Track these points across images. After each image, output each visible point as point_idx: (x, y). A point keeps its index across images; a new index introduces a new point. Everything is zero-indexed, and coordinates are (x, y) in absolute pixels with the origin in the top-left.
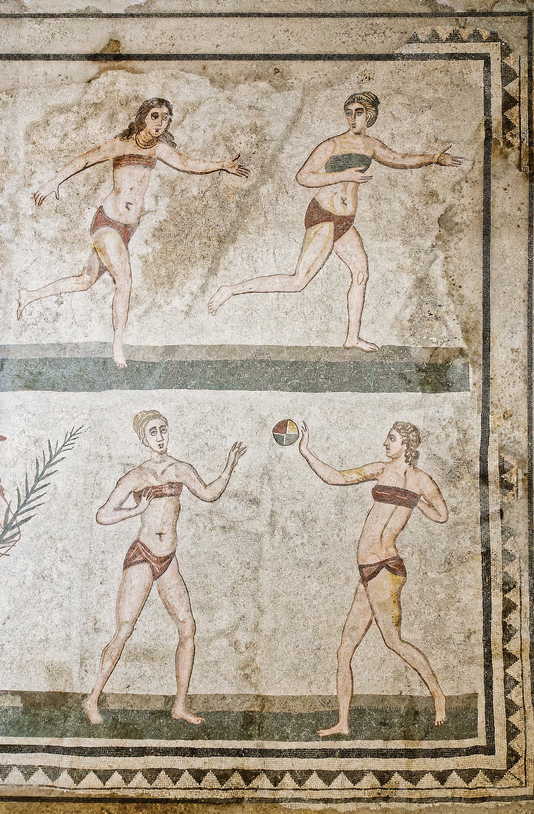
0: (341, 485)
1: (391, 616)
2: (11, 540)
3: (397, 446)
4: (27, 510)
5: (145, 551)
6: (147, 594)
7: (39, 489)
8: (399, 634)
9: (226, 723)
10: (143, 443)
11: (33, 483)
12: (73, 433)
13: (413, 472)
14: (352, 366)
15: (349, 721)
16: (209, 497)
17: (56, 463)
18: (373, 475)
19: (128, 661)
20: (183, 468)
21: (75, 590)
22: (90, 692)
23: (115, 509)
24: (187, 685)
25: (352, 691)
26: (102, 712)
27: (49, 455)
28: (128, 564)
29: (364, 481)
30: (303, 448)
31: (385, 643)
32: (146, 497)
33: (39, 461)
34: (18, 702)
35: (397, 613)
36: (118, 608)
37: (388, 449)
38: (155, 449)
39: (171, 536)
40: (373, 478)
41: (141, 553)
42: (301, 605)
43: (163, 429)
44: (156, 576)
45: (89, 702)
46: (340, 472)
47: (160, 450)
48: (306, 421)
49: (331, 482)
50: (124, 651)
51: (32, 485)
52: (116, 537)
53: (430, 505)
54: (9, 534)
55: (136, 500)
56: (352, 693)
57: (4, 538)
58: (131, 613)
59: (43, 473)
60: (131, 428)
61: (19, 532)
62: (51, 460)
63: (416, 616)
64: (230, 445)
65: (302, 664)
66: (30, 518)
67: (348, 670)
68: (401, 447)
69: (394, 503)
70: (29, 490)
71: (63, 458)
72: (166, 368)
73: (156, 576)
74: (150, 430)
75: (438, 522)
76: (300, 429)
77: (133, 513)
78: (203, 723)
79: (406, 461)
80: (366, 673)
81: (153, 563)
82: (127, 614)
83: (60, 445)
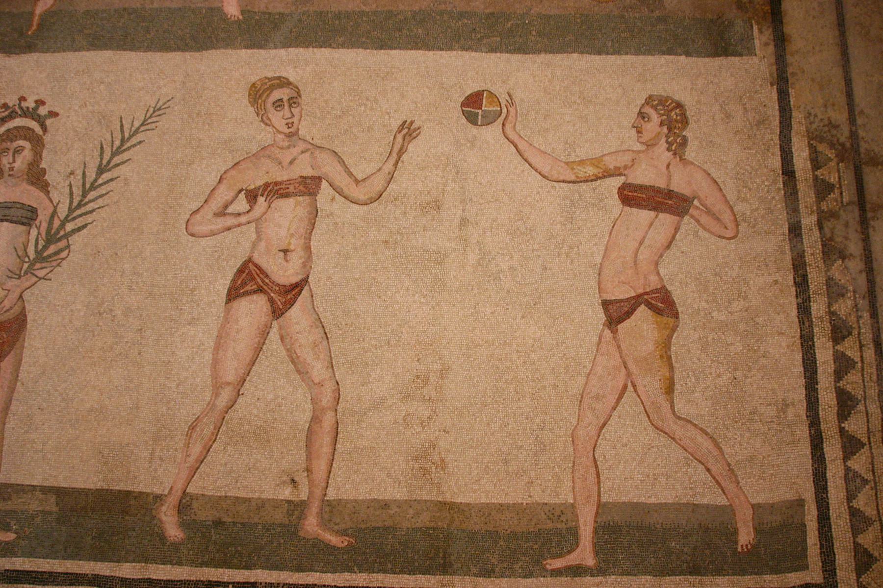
0: (569, 182)
1: (657, 378)
2: (55, 258)
3: (653, 127)
4: (80, 216)
5: (261, 275)
6: (262, 341)
8: (672, 407)
9: (389, 547)
10: (262, 121)
11: (94, 176)
12: (158, 107)
13: (681, 166)
14: (579, 20)
15: (595, 545)
16: (362, 198)
17: (129, 148)
18: (619, 168)
19: (228, 444)
20: (324, 158)
21: (148, 333)
22: (166, 492)
24: (324, 485)
25: (599, 496)
26: (183, 525)
27: (120, 137)
28: (234, 294)
29: (604, 177)
31: (650, 421)
32: (265, 196)
33: (105, 146)
34: (51, 505)
35: (667, 374)
36: (215, 363)
37: (639, 132)
38: (281, 129)
39: (302, 253)
40: (616, 172)
41: (254, 279)
42: (511, 361)
43: (293, 102)
44: (277, 312)
45: (164, 508)
46: (567, 163)
47: (287, 131)
48: (511, 91)
49: (554, 178)
50: (223, 428)
51: (92, 179)
52: (216, 255)
53: (709, 212)
54: (52, 249)
55: (249, 202)
56: (599, 500)
57: (45, 254)
58: (236, 369)
59: (109, 162)
60: (246, 101)
61: (68, 246)
62: (122, 145)
63: (697, 379)
64: (395, 124)
65: (515, 452)
67: (590, 463)
68: (658, 129)
69: (654, 209)
70: (88, 186)
71: (140, 142)
72: (300, 21)
73: (277, 312)
74: (273, 104)
75: (724, 238)
76: (503, 103)
77: (243, 219)
78: (350, 544)
79: (668, 150)
80: (621, 467)
81: (272, 295)
82: (230, 374)
83: (137, 124)
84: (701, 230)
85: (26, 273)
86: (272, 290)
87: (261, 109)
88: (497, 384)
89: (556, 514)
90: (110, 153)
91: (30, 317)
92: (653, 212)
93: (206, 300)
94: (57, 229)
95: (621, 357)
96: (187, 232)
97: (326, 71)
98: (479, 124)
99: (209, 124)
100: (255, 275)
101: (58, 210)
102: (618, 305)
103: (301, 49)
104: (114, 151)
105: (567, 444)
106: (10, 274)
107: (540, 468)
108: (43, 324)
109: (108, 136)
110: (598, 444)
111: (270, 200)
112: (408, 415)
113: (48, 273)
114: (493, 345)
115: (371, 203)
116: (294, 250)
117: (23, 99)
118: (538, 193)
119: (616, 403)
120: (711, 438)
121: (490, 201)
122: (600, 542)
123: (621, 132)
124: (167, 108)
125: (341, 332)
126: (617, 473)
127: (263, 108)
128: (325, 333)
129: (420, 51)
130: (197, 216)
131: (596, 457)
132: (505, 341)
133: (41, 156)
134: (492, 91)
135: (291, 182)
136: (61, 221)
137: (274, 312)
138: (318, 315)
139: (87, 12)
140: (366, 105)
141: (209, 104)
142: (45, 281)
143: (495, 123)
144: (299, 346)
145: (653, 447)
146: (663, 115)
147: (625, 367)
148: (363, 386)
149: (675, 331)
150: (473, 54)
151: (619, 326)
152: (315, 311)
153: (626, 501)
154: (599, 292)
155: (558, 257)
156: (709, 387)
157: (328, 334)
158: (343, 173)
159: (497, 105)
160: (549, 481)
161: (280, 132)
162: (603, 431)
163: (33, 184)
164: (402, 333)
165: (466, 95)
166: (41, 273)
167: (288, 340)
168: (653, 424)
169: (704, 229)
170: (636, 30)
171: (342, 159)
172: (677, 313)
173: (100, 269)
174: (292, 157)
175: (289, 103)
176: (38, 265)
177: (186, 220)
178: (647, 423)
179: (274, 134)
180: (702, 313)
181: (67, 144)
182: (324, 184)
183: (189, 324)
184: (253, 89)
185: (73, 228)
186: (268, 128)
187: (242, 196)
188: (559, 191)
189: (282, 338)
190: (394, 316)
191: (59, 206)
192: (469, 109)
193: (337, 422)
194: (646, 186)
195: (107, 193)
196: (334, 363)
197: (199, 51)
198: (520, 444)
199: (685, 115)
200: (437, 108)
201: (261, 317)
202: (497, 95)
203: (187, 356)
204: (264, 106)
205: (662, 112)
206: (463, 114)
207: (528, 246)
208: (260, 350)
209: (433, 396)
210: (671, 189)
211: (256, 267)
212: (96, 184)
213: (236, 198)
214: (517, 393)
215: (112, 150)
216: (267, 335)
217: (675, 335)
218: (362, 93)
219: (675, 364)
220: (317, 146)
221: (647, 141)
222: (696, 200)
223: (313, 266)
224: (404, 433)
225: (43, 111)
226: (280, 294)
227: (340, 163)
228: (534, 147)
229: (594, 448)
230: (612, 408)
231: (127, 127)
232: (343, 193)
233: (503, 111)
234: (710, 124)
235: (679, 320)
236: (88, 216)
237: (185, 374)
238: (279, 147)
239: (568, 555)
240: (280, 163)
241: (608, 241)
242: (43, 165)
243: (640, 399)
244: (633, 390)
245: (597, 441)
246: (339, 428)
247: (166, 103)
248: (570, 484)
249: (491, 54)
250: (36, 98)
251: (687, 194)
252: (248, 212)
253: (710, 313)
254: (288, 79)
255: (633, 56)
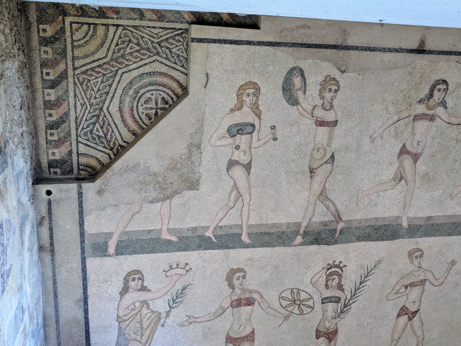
4: (354, 298)
10: (411, 263)
11: (359, 285)
17: (370, 275)
23: (395, 294)
28: (399, 315)
38: (417, 265)
41: (404, 311)
43: (421, 256)
44: (410, 319)
47: (417, 265)
51: (358, 286)
52: (394, 305)
54: (346, 309)
57: (343, 311)
59: (363, 280)
62: (368, 274)
64: (450, 261)
66: (356, 301)
70: (357, 289)
71: (373, 273)
73: (410, 319)
77: (403, 294)
82: (396, 337)
83: (372, 267)
85: (337, 317)
91: (339, 330)
101: (347, 297)
106: (332, 318)
109: (363, 272)
117: (334, 261)
133: (341, 280)
137: (409, 319)
139: (356, 228)
140: (442, 255)
161: (416, 266)
163: (339, 290)
166: (342, 317)
176: (341, 314)
181: (350, 276)
182: (427, 281)
187: (403, 287)
189: (411, 326)
225: (342, 265)
226: (411, 314)
231: (369, 268)
237: (384, 339)
242: (342, 283)
250: (339, 261)
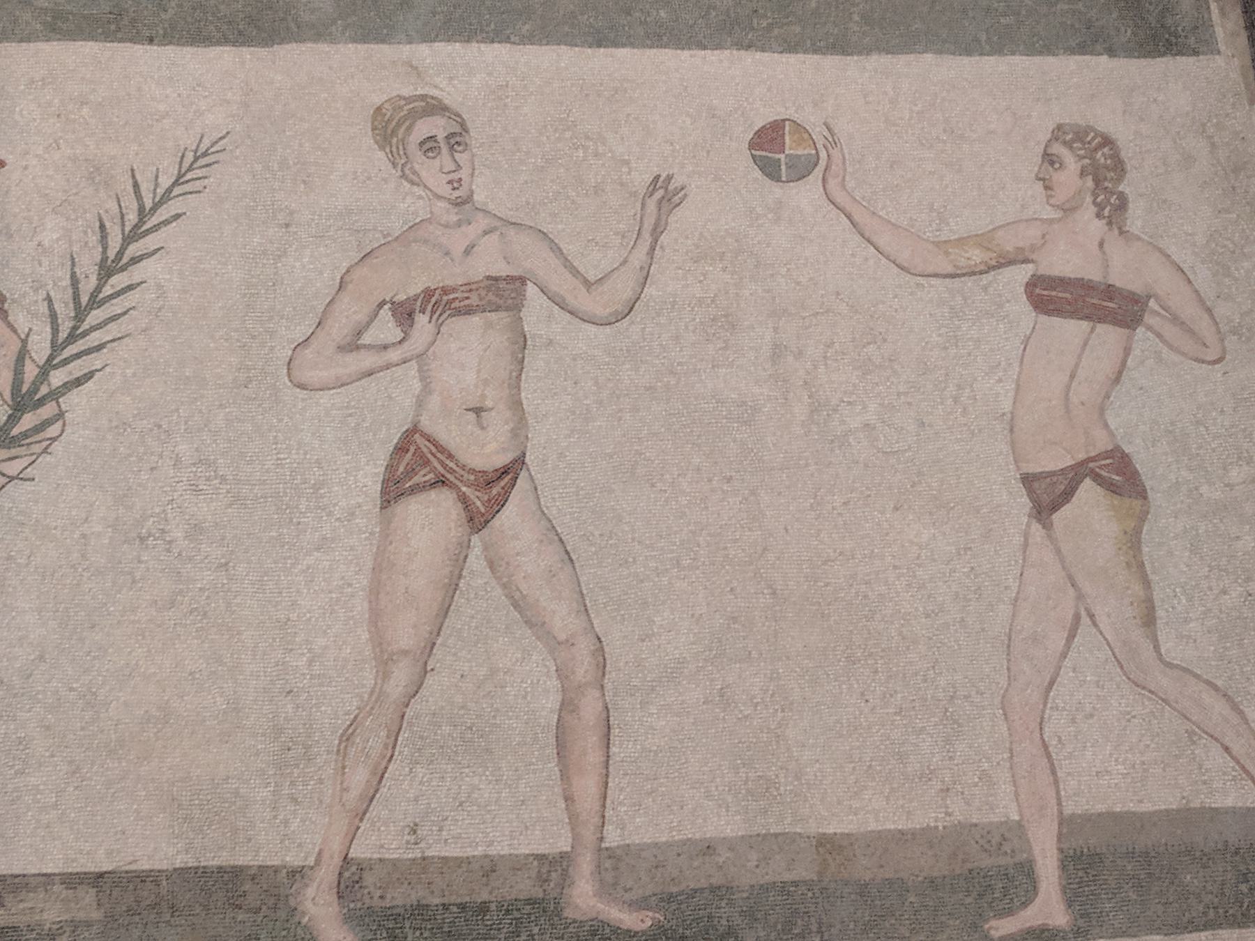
7: (111, 297)
11: (93, 280)
27: (135, 206)
30: (833, 184)
33: (108, 225)
48: (830, 121)
56: (1060, 812)
59: (120, 254)
84: (1165, 350)
86: (462, 481)
87: (399, 154)
88: (869, 623)
89: (994, 842)
90: (121, 236)
92: (1086, 323)
93: (343, 503)
94: (34, 383)
95: (1064, 568)
96: (291, 381)
97: (507, 86)
98: (784, 179)
99: (304, 182)
100: (429, 456)
102: (1048, 479)
103: (457, 44)
104: (126, 233)
105: (996, 720)
107: (957, 765)
108: (27, 565)
110: (1046, 716)
111: (438, 319)
112: (727, 686)
113: (26, 468)
114: (853, 558)
115: (617, 321)
116: (492, 409)
118: (896, 296)
119: (1065, 645)
120: (1224, 695)
121: (817, 313)
122: (1070, 884)
123: (1020, 190)
124: (221, 151)
125: (593, 549)
126: (1084, 765)
127: (401, 153)
128: (567, 553)
129: (667, 50)
130: (307, 351)
131: (1046, 739)
132: (873, 551)
134: (798, 121)
135: (474, 287)
136: (38, 366)
138: (550, 521)
141: (301, 145)
142: (21, 482)
143: (810, 177)
144: (524, 577)
145: (1134, 717)
146: (1085, 157)
147: (1073, 586)
148: (643, 641)
149: (1144, 521)
150: (758, 55)
151: (1054, 516)
152: (544, 514)
153: (1104, 810)
154: (1016, 462)
155: (942, 403)
156: (1210, 610)
157: (572, 555)
158: (562, 269)
159: (809, 146)
160: (976, 785)
162: (1052, 694)
164: (699, 546)
165: (756, 129)
167: (502, 569)
168: (1129, 679)
169: (1171, 347)
170: (1024, 13)
171: (556, 244)
172: (1145, 491)
173: (130, 455)
174: (468, 243)
175: (449, 143)
177: (288, 359)
178: (1120, 676)
179: (430, 200)
180: (1184, 489)
183: (318, 549)
184: (379, 118)
185: (66, 380)
186: (415, 189)
188: (929, 292)
190: (681, 518)
191: (30, 339)
192: (764, 153)
193: (607, 707)
194: (1070, 279)
195: (125, 313)
196: (589, 605)
197: (266, 45)
198: (920, 725)
199: (1118, 156)
200: (708, 152)
201: (450, 529)
202: (808, 128)
203: (319, 608)
204: (404, 149)
205: (1082, 152)
206: (755, 161)
207: (889, 387)
208: (456, 589)
209: (764, 652)
210: (1110, 282)
211: (429, 441)
212: (101, 296)
213: (375, 317)
214: (903, 638)
215: (123, 230)
216: (465, 562)
217: (1145, 528)
218: (576, 126)
219: (1151, 577)
220: (509, 222)
221: (1064, 203)
222: (1152, 300)
223: (530, 436)
224: (724, 718)
227: (553, 251)
228: (880, 217)
229: (1041, 724)
230: (1061, 654)
232: (567, 305)
233: (821, 155)
234: (1160, 171)
235: (1149, 502)
236: (93, 355)
238: (442, 225)
239: (1022, 910)
240: (447, 254)
241: (1020, 373)
243: (1104, 637)
244: (1090, 623)
245: (1043, 712)
246: (611, 719)
247: (216, 142)
248: (1010, 788)
249: (788, 55)
251: (1138, 292)
252: (400, 342)
253: (1197, 488)
254: (440, 101)
255: (1024, 58)
